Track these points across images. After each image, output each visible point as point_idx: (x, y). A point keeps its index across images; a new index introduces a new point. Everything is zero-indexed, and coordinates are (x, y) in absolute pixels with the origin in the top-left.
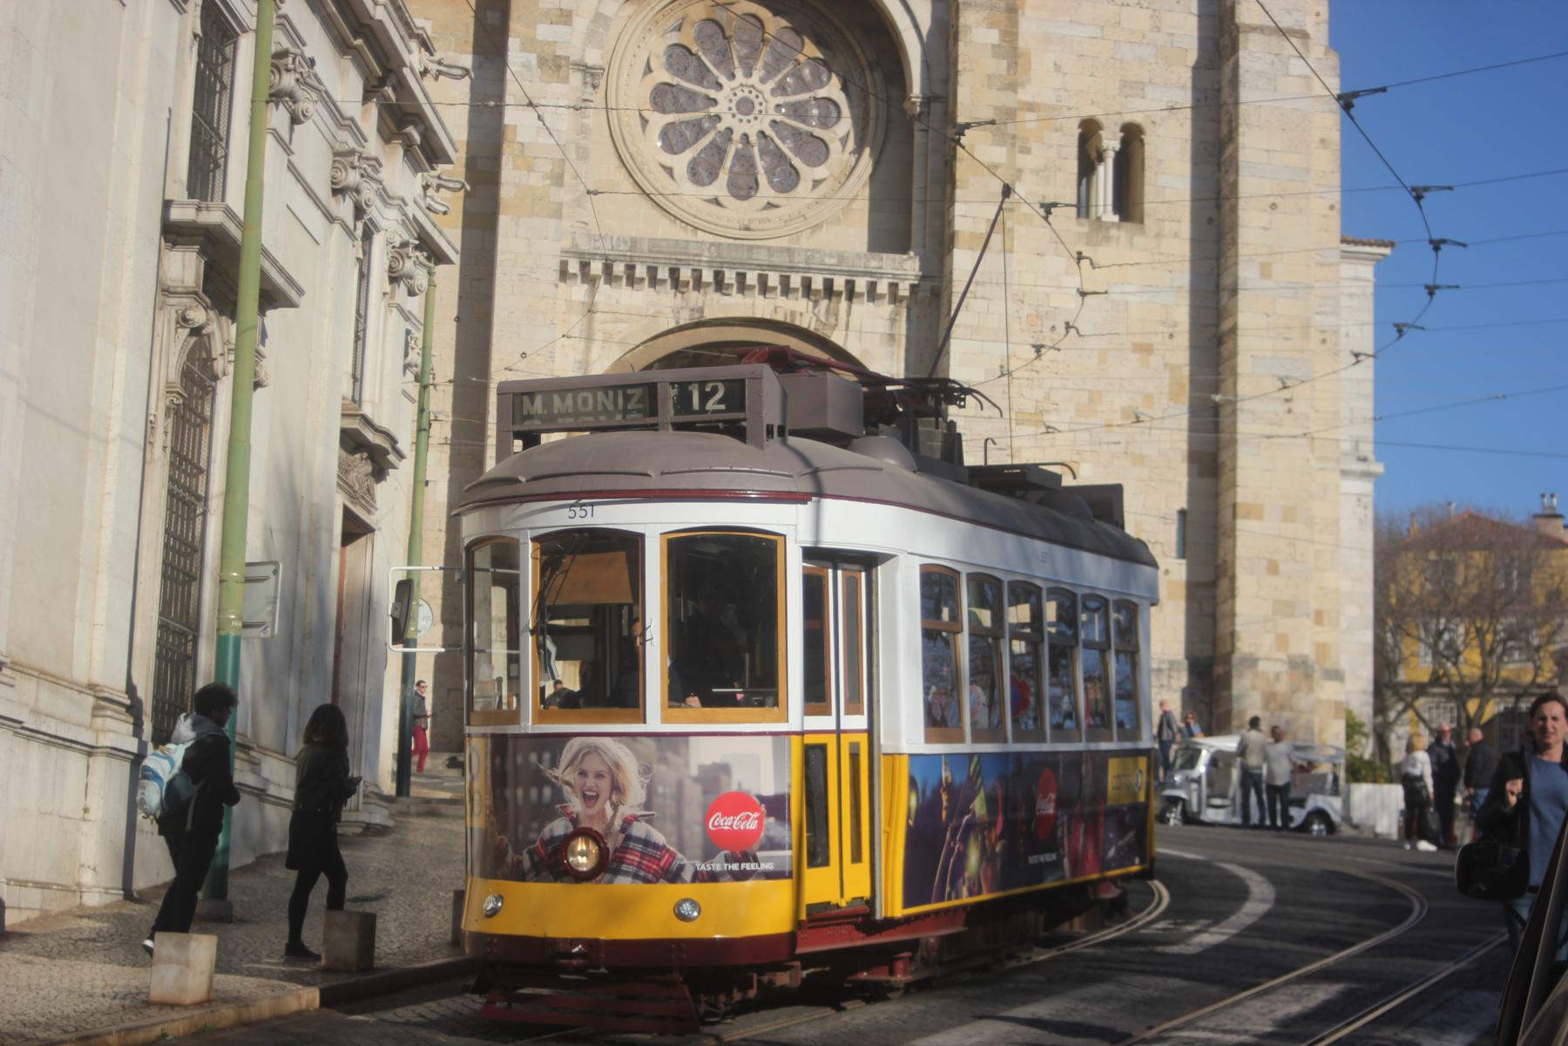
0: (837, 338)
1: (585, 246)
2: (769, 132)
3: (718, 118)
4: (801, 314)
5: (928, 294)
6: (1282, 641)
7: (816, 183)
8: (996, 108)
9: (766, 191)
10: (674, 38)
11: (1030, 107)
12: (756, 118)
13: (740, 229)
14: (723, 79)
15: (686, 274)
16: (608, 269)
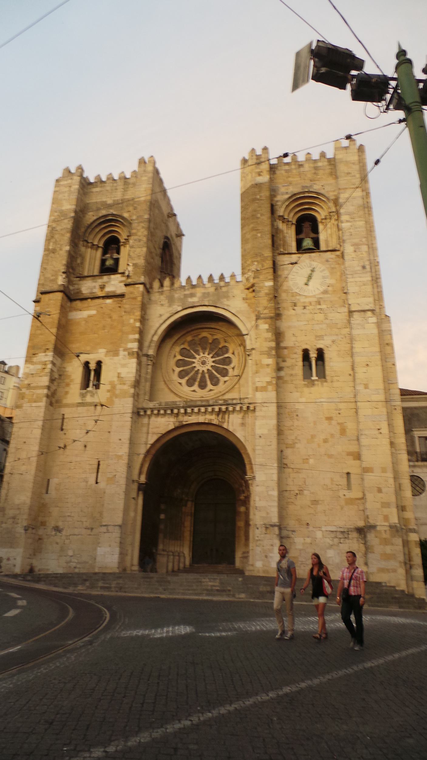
0: (225, 426)
1: (145, 406)
2: (210, 369)
3: (195, 367)
4: (214, 420)
5: (253, 409)
6: (386, 518)
7: (225, 382)
8: (269, 348)
9: (210, 386)
10: (182, 347)
11: (285, 348)
12: (207, 366)
13: (201, 398)
14: (197, 356)
15: (176, 411)
16: (152, 411)
